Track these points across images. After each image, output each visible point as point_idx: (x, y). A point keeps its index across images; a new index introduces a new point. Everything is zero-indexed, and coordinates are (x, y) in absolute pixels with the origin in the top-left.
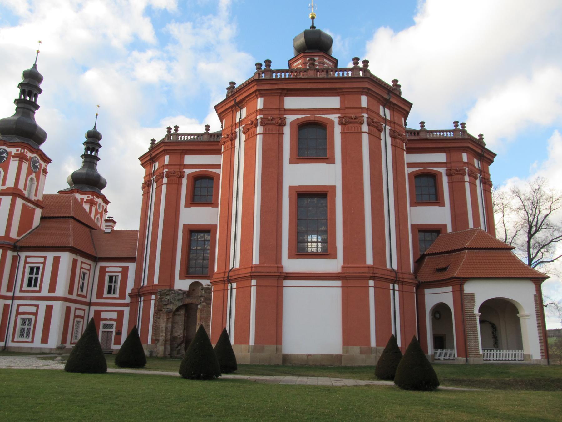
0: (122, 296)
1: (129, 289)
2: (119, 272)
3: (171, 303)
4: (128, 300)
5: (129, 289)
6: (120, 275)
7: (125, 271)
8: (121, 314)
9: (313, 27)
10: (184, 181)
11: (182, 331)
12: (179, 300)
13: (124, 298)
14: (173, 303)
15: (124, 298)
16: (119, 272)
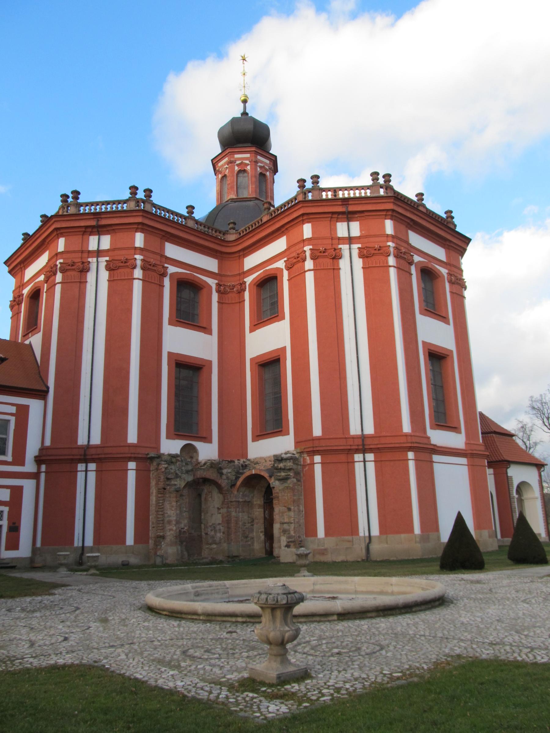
0: (19, 459)
1: (32, 448)
2: (12, 414)
3: (177, 476)
4: (30, 467)
5: (32, 448)
6: (13, 419)
7: (22, 414)
8: (17, 492)
9: (245, 114)
10: (167, 282)
11: (186, 521)
12: (187, 472)
13: (23, 464)
14: (180, 477)
15: (23, 464)
16: (12, 414)
